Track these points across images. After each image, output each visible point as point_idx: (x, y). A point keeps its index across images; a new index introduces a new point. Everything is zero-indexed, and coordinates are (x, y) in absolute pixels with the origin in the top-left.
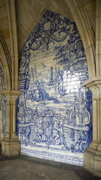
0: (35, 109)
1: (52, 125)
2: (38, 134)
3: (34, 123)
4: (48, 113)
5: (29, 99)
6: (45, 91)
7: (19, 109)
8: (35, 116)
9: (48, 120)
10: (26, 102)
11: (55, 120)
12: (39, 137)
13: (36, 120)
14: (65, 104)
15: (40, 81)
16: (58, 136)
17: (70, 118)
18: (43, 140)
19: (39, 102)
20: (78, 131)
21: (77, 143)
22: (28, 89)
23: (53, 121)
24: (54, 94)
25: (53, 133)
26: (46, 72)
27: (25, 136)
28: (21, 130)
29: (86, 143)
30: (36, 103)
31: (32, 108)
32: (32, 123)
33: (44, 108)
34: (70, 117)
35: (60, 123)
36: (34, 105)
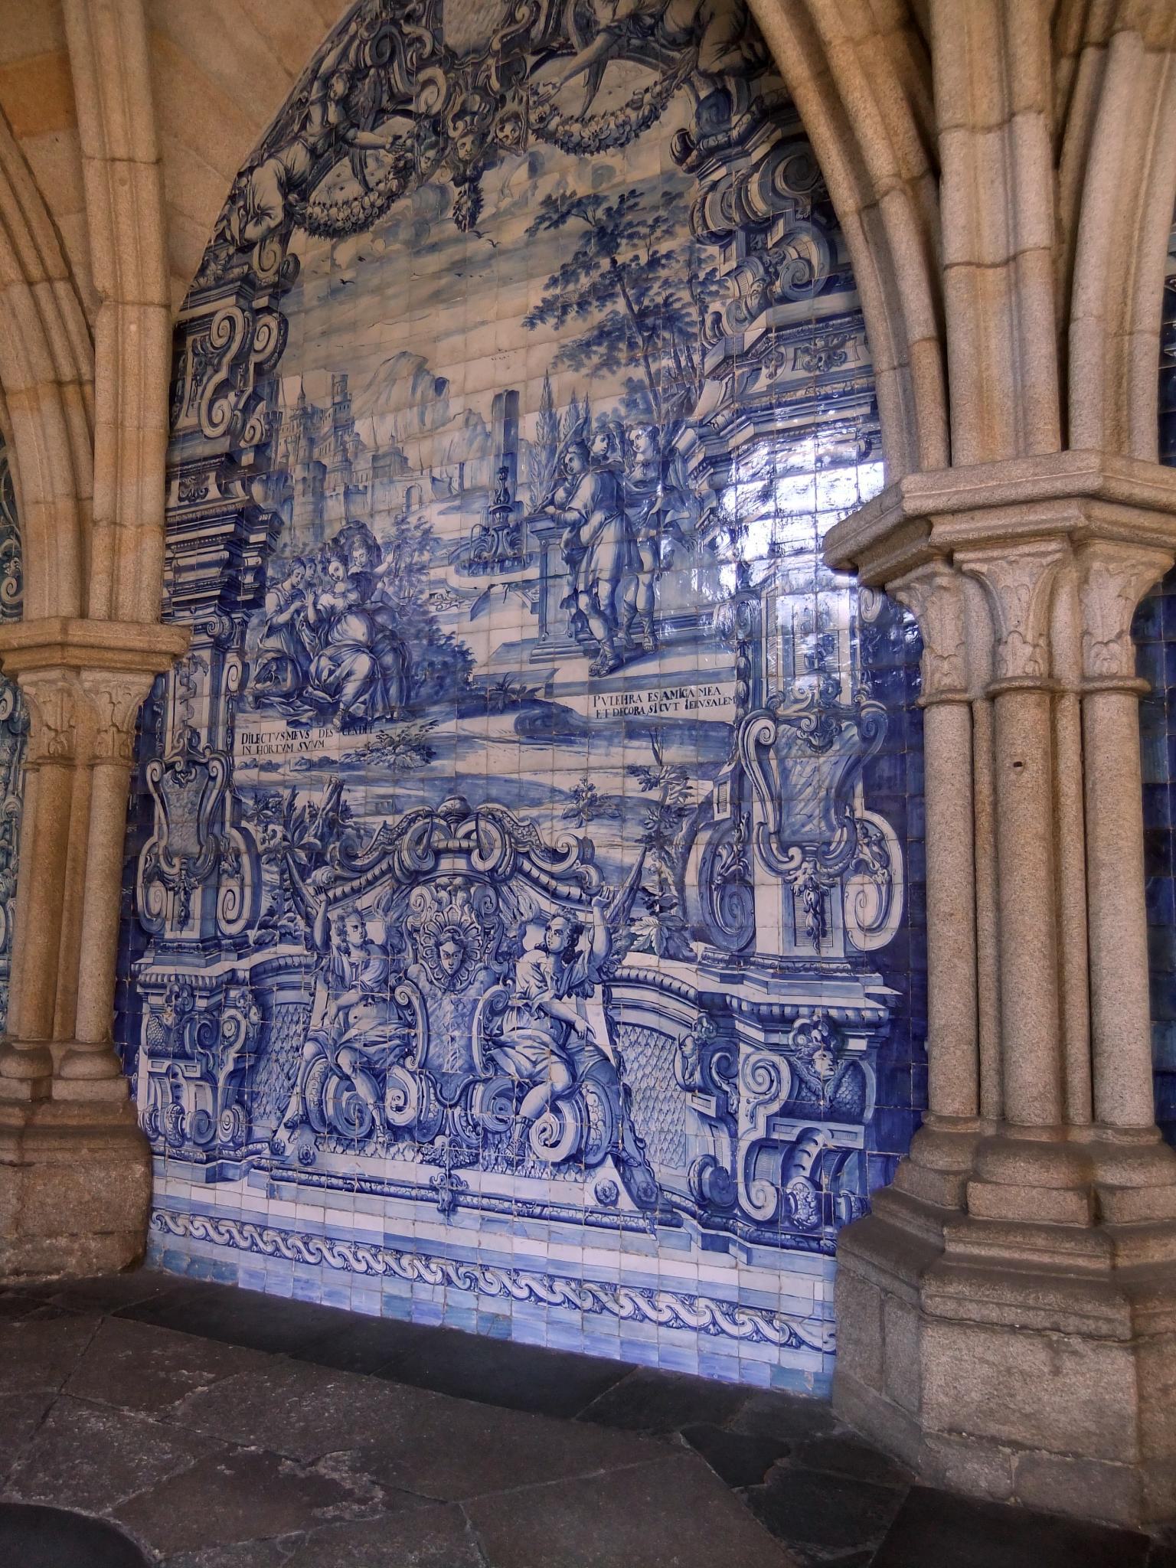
0: (320, 798)
1: (496, 968)
2: (345, 1060)
3: (311, 946)
4: (453, 844)
5: (260, 702)
6: (432, 621)
7: (158, 810)
8: (321, 875)
9: (459, 912)
10: (231, 731)
11: (528, 915)
12: (351, 1088)
13: (333, 915)
14: (640, 753)
15: (381, 529)
16: (559, 1077)
17: (692, 893)
18: (399, 1119)
19: (371, 737)
20: (775, 1021)
21: (762, 1146)
22: (257, 603)
23: (506, 917)
24: (526, 656)
25: (501, 1045)
26: (453, 439)
27: (209, 1077)
28: (169, 1019)
29: (859, 1144)
30: (334, 743)
31: (286, 793)
32: (285, 949)
33: (413, 793)
34: (691, 877)
35: (583, 944)
36: (311, 765)
